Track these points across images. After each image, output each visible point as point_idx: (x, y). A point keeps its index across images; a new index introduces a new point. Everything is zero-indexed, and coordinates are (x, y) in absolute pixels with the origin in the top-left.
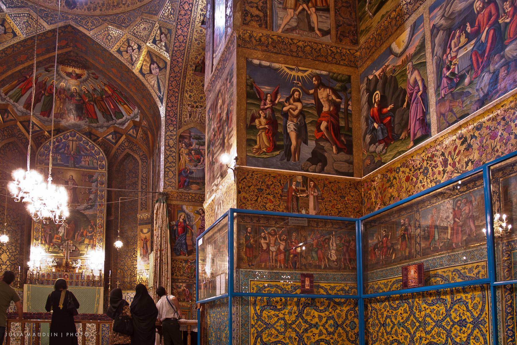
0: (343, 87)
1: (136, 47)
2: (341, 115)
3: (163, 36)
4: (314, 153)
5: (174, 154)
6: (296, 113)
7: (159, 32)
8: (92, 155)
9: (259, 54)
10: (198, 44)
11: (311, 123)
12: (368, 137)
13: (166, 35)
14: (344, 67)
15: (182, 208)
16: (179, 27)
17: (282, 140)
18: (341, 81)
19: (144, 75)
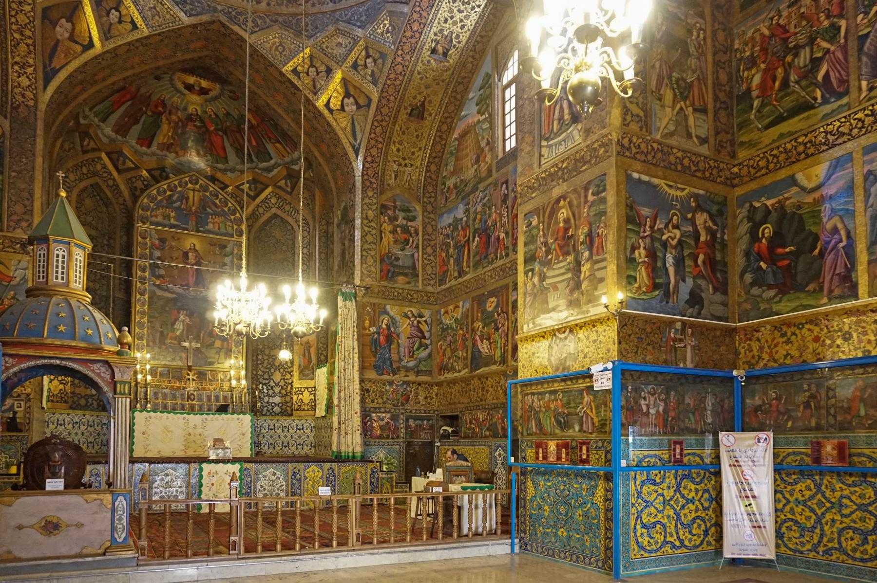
0: (719, 212)
1: (323, 68)
2: (718, 247)
3: (369, 60)
4: (692, 293)
5: (374, 231)
6: (674, 243)
7: (364, 53)
8: (224, 214)
9: (638, 165)
10: (421, 79)
11: (688, 255)
12: (748, 277)
13: (375, 61)
14: (721, 186)
15: (385, 308)
16: (400, 52)
17: (660, 277)
18: (718, 203)
19: (331, 111)
